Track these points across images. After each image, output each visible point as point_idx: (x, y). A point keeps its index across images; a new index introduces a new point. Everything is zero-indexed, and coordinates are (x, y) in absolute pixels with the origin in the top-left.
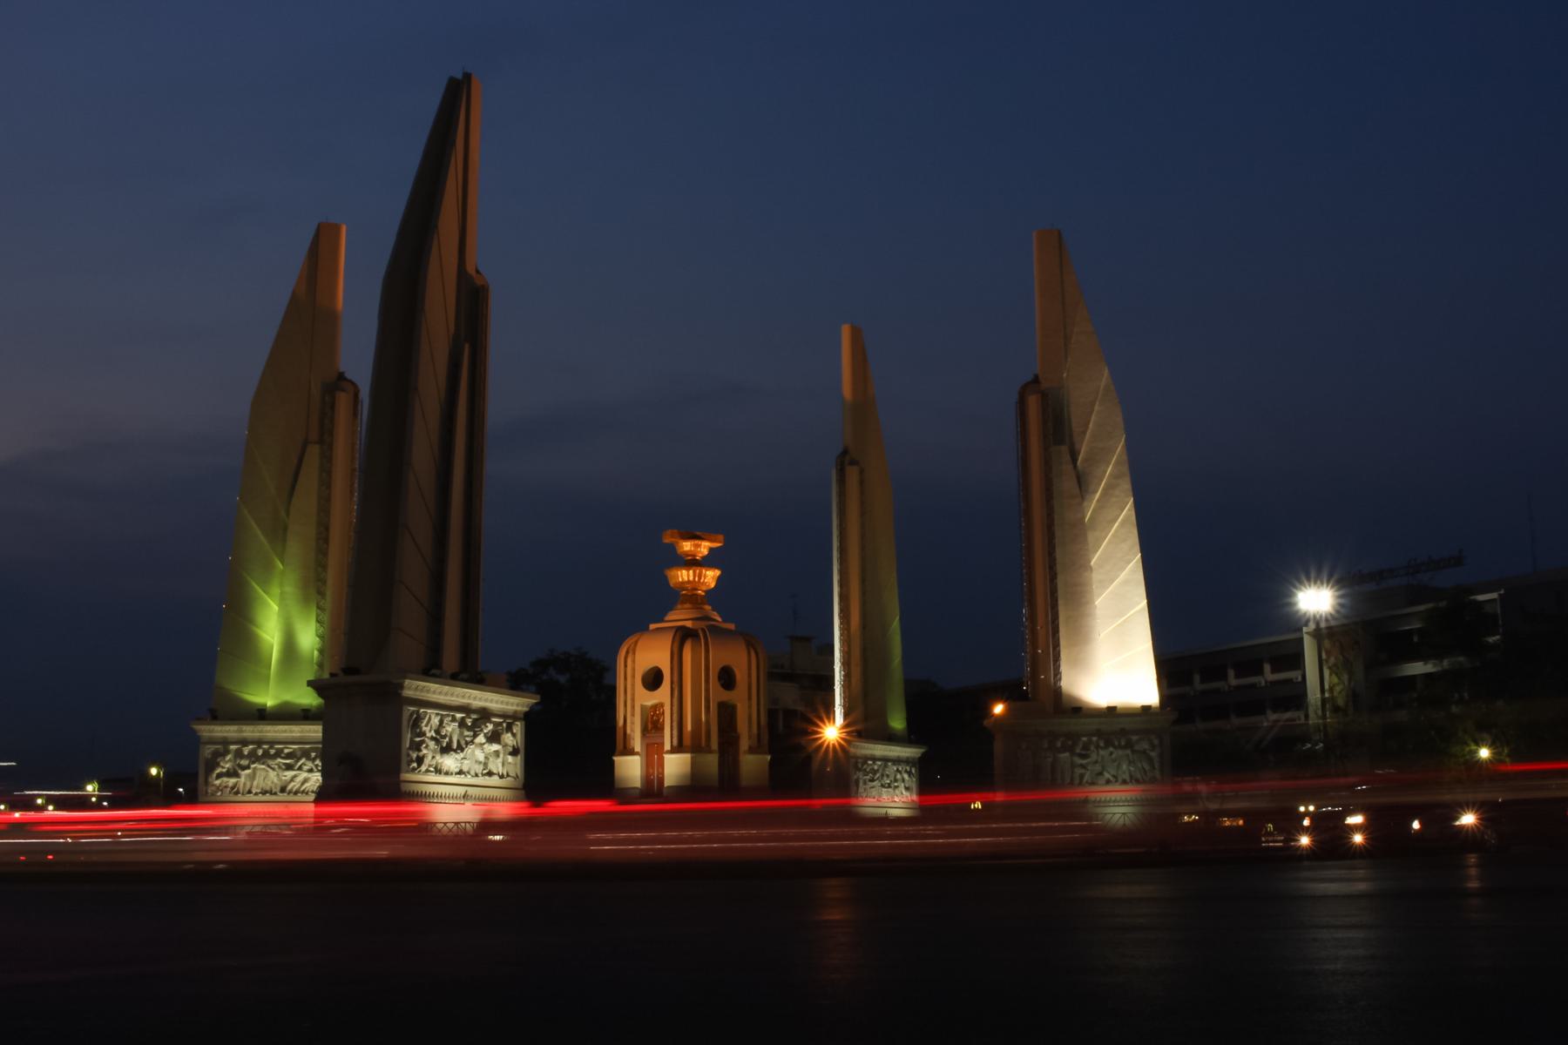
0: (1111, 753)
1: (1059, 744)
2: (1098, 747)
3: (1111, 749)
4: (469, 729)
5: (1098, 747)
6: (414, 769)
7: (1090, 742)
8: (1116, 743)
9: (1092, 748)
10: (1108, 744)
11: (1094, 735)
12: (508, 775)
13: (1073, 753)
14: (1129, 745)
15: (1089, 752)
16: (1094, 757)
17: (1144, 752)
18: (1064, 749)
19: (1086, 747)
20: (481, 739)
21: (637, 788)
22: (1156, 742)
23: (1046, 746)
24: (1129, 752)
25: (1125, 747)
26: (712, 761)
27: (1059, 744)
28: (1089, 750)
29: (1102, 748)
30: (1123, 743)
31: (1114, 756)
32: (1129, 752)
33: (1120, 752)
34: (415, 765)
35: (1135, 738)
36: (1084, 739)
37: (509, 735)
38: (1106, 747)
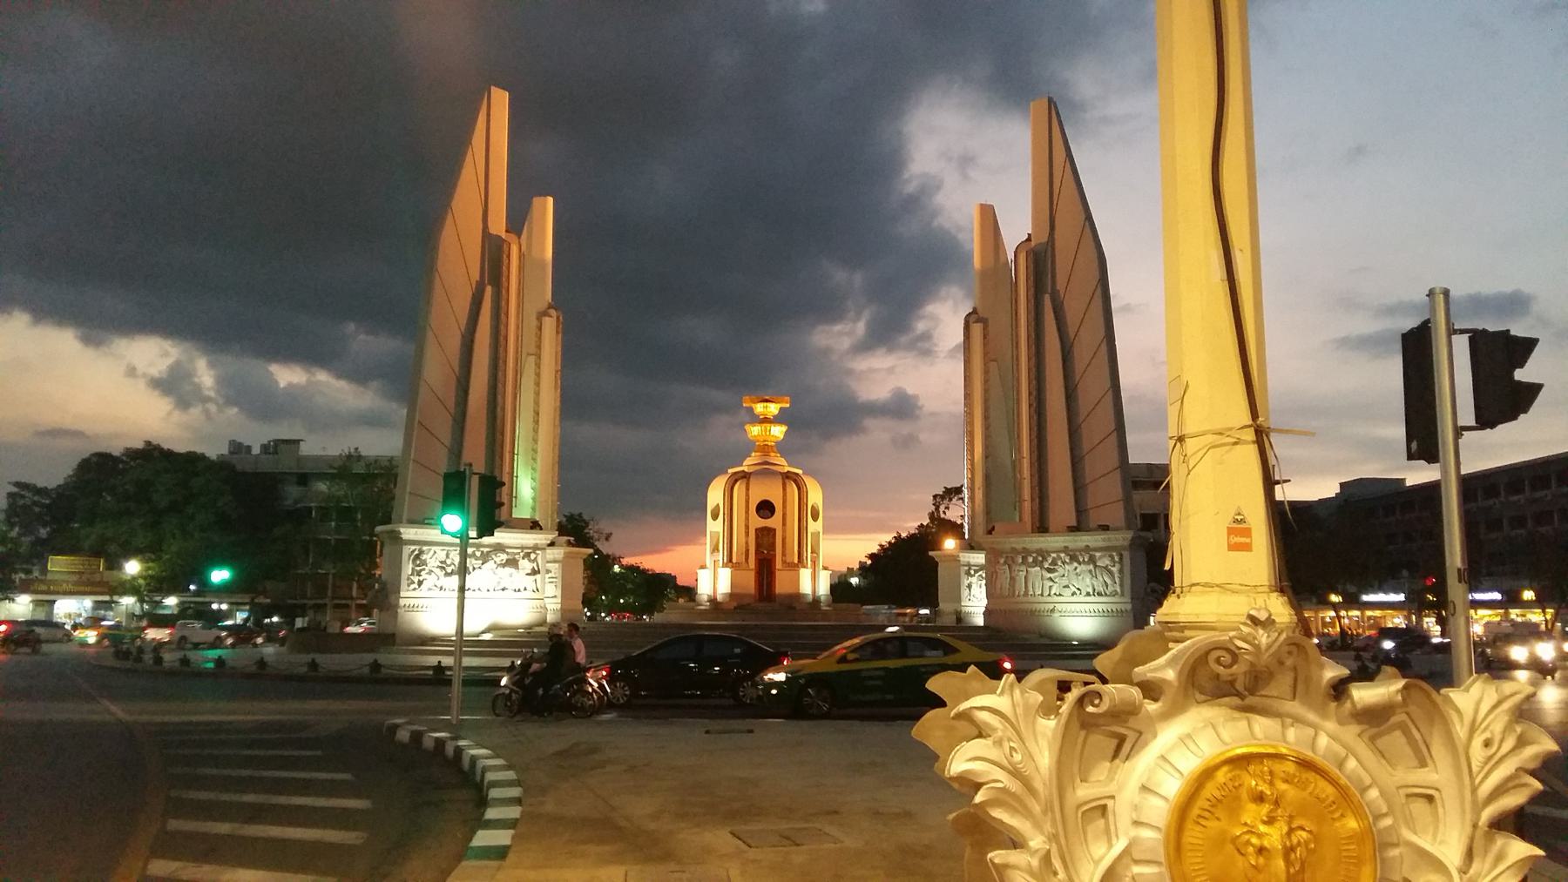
0: (1076, 569)
1: (1031, 560)
2: (1064, 563)
3: (1075, 564)
4: (477, 559)
5: (1064, 563)
6: (415, 589)
7: (1058, 556)
8: (1081, 560)
9: (1060, 563)
10: (1073, 558)
11: (1060, 552)
12: (525, 589)
13: (1042, 567)
14: (1092, 560)
15: (1056, 567)
16: (1061, 571)
17: (1106, 568)
18: (1036, 563)
19: (1054, 563)
20: (490, 564)
21: (750, 595)
22: (1117, 559)
23: (1020, 561)
24: (1091, 567)
25: (1088, 563)
26: (749, 581)
27: (1031, 560)
28: (1056, 564)
29: (1068, 564)
30: (1086, 560)
31: (1078, 571)
32: (1091, 567)
33: (1083, 567)
34: (416, 586)
35: (1098, 554)
36: (1054, 555)
37: (526, 560)
38: (1071, 563)
